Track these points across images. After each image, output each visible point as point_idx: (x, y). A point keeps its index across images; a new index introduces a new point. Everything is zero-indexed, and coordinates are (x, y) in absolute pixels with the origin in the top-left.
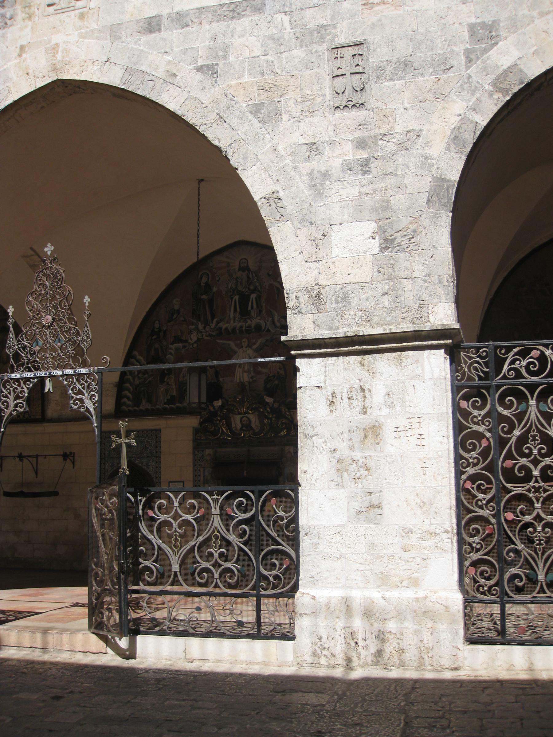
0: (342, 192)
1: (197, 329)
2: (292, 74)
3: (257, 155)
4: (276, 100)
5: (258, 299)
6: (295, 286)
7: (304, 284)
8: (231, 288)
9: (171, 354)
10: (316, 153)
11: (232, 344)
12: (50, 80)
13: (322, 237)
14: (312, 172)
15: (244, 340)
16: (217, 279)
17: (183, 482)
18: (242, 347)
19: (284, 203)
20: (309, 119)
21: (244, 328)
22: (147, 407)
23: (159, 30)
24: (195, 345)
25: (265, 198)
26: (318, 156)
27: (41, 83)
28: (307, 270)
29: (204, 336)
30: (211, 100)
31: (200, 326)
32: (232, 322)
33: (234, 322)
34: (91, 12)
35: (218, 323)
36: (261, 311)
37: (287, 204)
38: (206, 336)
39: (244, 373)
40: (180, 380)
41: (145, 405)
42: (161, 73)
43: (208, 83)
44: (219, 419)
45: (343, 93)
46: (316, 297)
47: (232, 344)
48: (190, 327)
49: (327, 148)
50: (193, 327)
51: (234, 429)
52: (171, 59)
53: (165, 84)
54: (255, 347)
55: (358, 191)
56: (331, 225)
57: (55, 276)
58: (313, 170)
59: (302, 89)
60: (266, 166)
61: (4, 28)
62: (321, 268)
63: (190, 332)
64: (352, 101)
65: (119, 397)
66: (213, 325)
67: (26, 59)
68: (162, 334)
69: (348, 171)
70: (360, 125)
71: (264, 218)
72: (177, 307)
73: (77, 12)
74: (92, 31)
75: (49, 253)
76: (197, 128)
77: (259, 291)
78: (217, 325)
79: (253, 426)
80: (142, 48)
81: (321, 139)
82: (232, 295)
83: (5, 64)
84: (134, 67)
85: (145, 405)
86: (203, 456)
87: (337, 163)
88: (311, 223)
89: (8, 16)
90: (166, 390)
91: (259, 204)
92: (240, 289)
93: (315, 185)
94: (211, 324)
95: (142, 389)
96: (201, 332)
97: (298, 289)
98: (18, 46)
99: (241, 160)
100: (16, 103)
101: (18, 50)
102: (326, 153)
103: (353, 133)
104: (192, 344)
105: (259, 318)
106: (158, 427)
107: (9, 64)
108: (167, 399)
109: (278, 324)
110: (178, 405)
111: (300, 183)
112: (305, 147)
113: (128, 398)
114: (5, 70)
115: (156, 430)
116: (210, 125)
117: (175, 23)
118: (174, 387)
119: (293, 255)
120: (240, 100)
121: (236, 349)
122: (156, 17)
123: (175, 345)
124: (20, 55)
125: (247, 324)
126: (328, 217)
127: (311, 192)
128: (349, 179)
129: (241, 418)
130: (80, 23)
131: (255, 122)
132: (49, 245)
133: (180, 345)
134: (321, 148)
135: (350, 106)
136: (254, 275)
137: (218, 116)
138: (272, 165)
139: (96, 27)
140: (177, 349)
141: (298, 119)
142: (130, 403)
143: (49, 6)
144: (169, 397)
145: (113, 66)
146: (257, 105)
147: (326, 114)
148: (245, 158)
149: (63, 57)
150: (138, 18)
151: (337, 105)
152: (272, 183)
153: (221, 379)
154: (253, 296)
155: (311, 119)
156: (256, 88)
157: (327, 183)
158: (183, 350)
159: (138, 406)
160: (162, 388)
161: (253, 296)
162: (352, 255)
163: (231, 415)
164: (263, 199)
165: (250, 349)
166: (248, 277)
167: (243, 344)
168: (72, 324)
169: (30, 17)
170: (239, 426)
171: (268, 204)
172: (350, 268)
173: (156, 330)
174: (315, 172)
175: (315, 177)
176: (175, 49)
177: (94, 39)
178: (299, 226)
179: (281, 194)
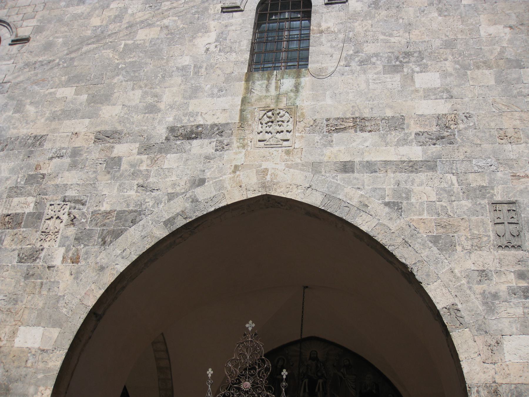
0: (509, 310)
2: (462, 218)
3: (437, 275)
4: (451, 235)
6: (475, 381)
7: (483, 381)
10: (486, 278)
12: (260, 194)
13: (496, 345)
14: (484, 293)
19: (463, 313)
20: (478, 252)
23: (353, 172)
25: (446, 308)
26: (487, 281)
27: (251, 195)
28: (485, 370)
30: (397, 228)
34: (296, 150)
37: (465, 315)
42: (355, 202)
43: (394, 215)
45: (503, 236)
46: (494, 392)
49: (495, 276)
52: (363, 194)
53: (358, 211)
55: (522, 311)
56: (502, 335)
57: (255, 349)
58: (484, 291)
59: (470, 230)
60: (445, 283)
61: (221, 151)
62: (497, 369)
64: (511, 243)
67: (239, 175)
69: (513, 295)
70: (519, 261)
71: (446, 324)
73: (284, 148)
74: (297, 164)
75: (250, 329)
76: (387, 247)
80: (339, 182)
81: (489, 268)
83: (221, 177)
84: (333, 195)
87: (503, 288)
88: (486, 332)
89: (225, 142)
91: (442, 313)
93: (487, 303)
97: (478, 385)
98: (233, 165)
99: (424, 277)
100: (228, 206)
101: (233, 168)
102: (494, 279)
103: (514, 266)
107: (224, 177)
111: (475, 300)
112: (477, 273)
114: (221, 180)
116: (397, 246)
117: (365, 169)
119: (472, 356)
120: (421, 231)
122: (349, 162)
124: (234, 172)
126: (500, 328)
127: (484, 307)
128: (515, 301)
130: (286, 157)
131: (435, 249)
132: (251, 322)
134: (490, 275)
135: (510, 246)
136: (322, 364)
137: (404, 241)
138: (450, 283)
139: (299, 161)
141: (469, 251)
143: (260, 141)
145: (314, 192)
146: (435, 237)
147: (492, 250)
148: (428, 275)
149: (272, 179)
150: (335, 161)
151: (500, 244)
152: (452, 297)
154: (320, 381)
155: (480, 252)
156: (433, 224)
157: (497, 302)
161: (320, 381)
162: (521, 361)
164: (444, 309)
168: (269, 392)
169: (244, 147)
171: (449, 314)
172: (521, 372)
174: (487, 292)
175: (486, 296)
176: (366, 187)
177: (298, 170)
178: (476, 334)
179: (460, 306)
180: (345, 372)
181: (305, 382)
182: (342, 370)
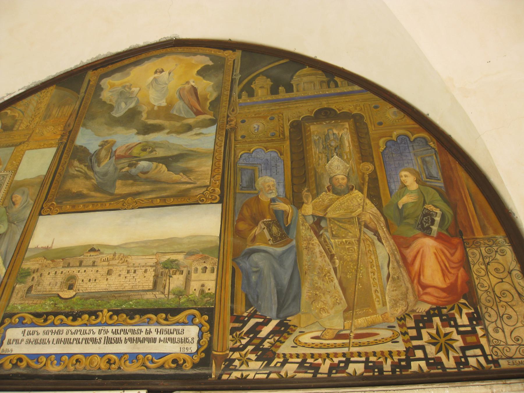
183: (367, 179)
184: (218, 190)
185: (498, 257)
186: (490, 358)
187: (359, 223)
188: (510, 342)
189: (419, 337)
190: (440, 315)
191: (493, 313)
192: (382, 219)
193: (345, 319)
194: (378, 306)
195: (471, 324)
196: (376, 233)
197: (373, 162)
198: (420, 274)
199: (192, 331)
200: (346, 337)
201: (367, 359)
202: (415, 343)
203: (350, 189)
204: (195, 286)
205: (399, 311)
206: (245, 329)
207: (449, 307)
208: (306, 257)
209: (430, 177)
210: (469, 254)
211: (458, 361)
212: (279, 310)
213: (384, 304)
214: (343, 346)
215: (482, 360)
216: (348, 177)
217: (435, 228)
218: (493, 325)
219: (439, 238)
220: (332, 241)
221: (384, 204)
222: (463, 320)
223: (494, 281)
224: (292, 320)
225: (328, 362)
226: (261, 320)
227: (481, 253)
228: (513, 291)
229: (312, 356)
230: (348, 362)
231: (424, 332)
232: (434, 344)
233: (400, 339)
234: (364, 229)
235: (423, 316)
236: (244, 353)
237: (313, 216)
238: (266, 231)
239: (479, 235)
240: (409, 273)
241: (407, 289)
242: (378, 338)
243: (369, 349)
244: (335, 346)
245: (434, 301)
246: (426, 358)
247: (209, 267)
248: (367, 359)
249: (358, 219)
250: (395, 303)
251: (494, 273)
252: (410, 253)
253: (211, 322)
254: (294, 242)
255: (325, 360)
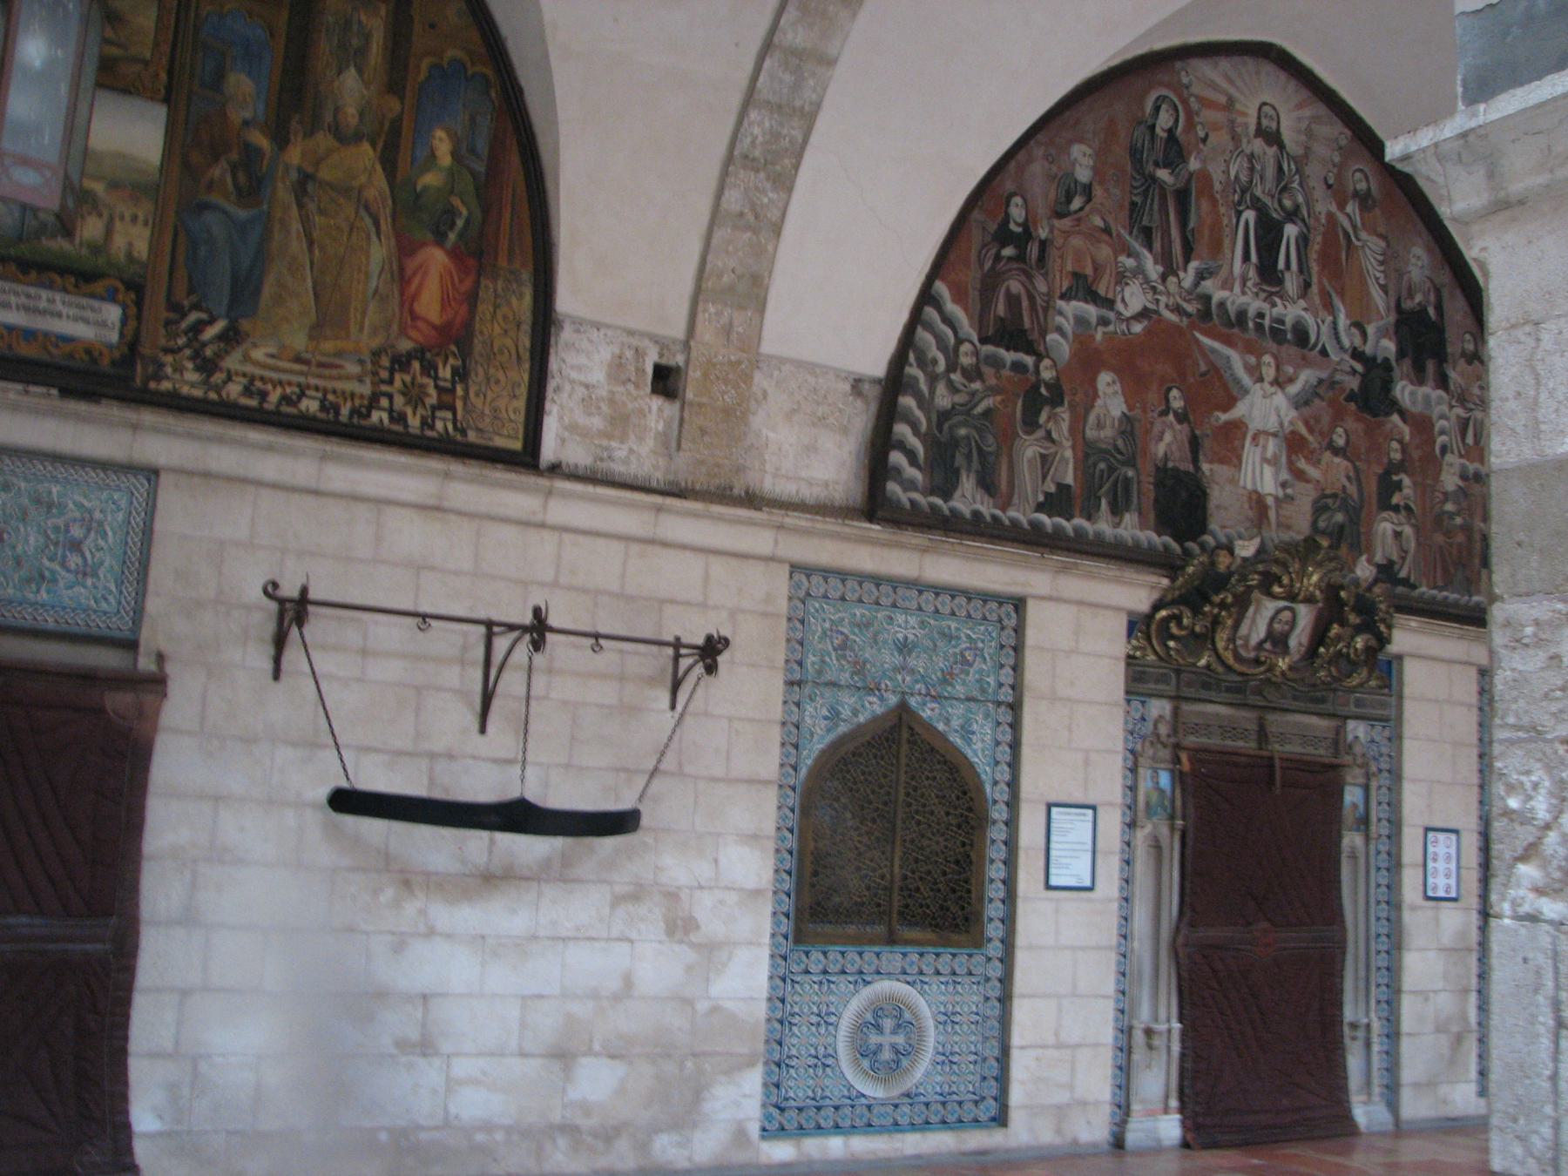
1: (1139, 271)
5: (1303, 241)
8: (1237, 177)
9: (1060, 330)
11: (1237, 361)
15: (1267, 358)
16: (1201, 134)
17: (1094, 808)
18: (1261, 379)
21: (1267, 322)
22: (978, 507)
24: (1138, 328)
29: (1162, 306)
31: (1153, 270)
32: (1237, 288)
33: (1244, 293)
35: (1201, 276)
36: (1307, 285)
38: (1167, 306)
39: (1265, 466)
40: (1090, 433)
41: (968, 499)
44: (1230, 599)
47: (1237, 361)
48: (1122, 258)
50: (1130, 263)
51: (1239, 642)
54: (1293, 389)
63: (1121, 278)
65: (880, 444)
66: (1188, 279)
68: (1033, 250)
72: (1083, 175)
77: (1303, 220)
78: (1196, 284)
79: (1293, 643)
82: (1239, 203)
85: (968, 499)
86: (1143, 719)
90: (1043, 457)
92: (1258, 192)
94: (1182, 274)
95: (963, 432)
96: (1154, 289)
104: (1128, 320)
105: (1302, 303)
106: (1016, 590)
108: (1047, 495)
109: (1346, 343)
110: (1079, 521)
113: (911, 456)
115: (1000, 599)
118: (1069, 454)
121: (1246, 380)
123: (1074, 303)
125: (1275, 311)
129: (1279, 611)
133: (1091, 311)
136: (1293, 167)
140: (1081, 321)
142: (912, 473)
144: (1052, 489)
153: (1205, 467)
154: (1291, 231)
158: (1101, 330)
159: (947, 495)
160: (1029, 449)
163: (1256, 594)
165: (1280, 393)
166: (1280, 169)
167: (1264, 370)
170: (1260, 632)
173: (1013, 227)
180: (1358, 219)
181: (1247, 223)
182: (1349, 209)
183: (387, 125)
184: (164, 76)
185: (514, 301)
186: (459, 425)
187: (359, 201)
188: (487, 411)
189: (391, 382)
190: (422, 360)
191: (480, 371)
192: (390, 202)
193: (311, 337)
194: (353, 329)
195: (454, 383)
196: (377, 224)
197: (402, 99)
198: (415, 297)
199: (113, 313)
200: (307, 362)
201: (325, 395)
202: (384, 388)
203: (358, 138)
204: (119, 242)
205: (376, 343)
206: (184, 325)
207: (436, 350)
208: (277, 235)
209: (472, 151)
210: (482, 286)
211: (424, 423)
212: (231, 307)
213: (361, 329)
214: (301, 373)
215: (450, 427)
216: (361, 115)
217: (452, 236)
218: (476, 388)
219: (454, 254)
220: (317, 218)
221: (399, 178)
222: (445, 373)
223: (497, 330)
224: (245, 325)
225: (279, 391)
226: (204, 316)
227: (495, 291)
228: (513, 351)
229: (262, 379)
230: (302, 395)
231: (398, 377)
232: (404, 394)
233: (368, 380)
234: (363, 213)
235: (402, 355)
236: (177, 357)
237: (300, 170)
238: (229, 180)
239: (502, 262)
240: (402, 294)
241: (394, 315)
242: (342, 372)
243: (329, 385)
244: (292, 372)
245: (421, 339)
246: (391, 411)
247: (141, 218)
248: (325, 395)
249: (359, 192)
250: (375, 331)
251: (501, 321)
252: (411, 265)
253: (139, 304)
254: (265, 207)
255: (274, 387)
